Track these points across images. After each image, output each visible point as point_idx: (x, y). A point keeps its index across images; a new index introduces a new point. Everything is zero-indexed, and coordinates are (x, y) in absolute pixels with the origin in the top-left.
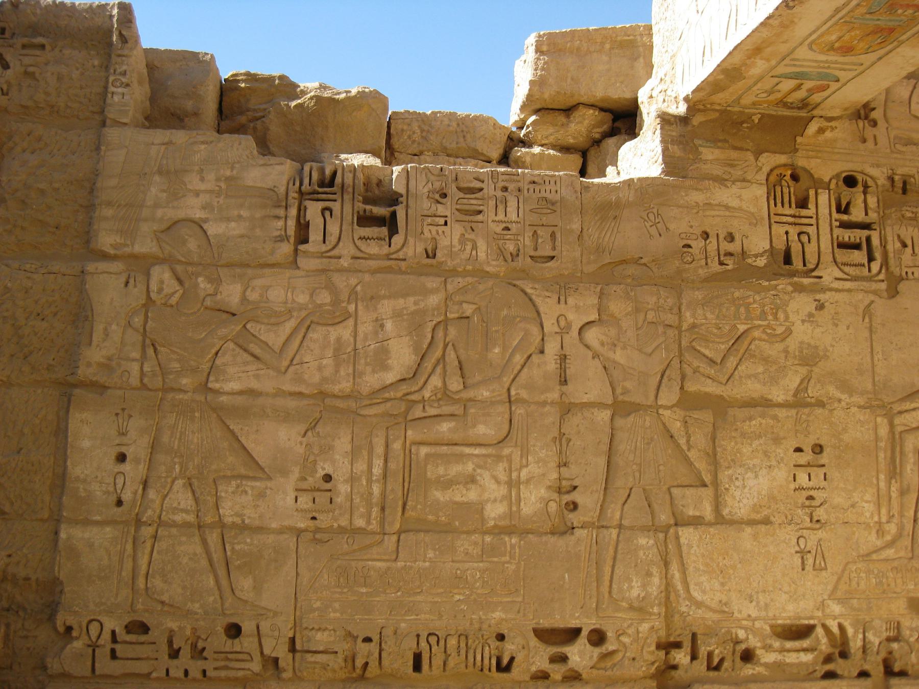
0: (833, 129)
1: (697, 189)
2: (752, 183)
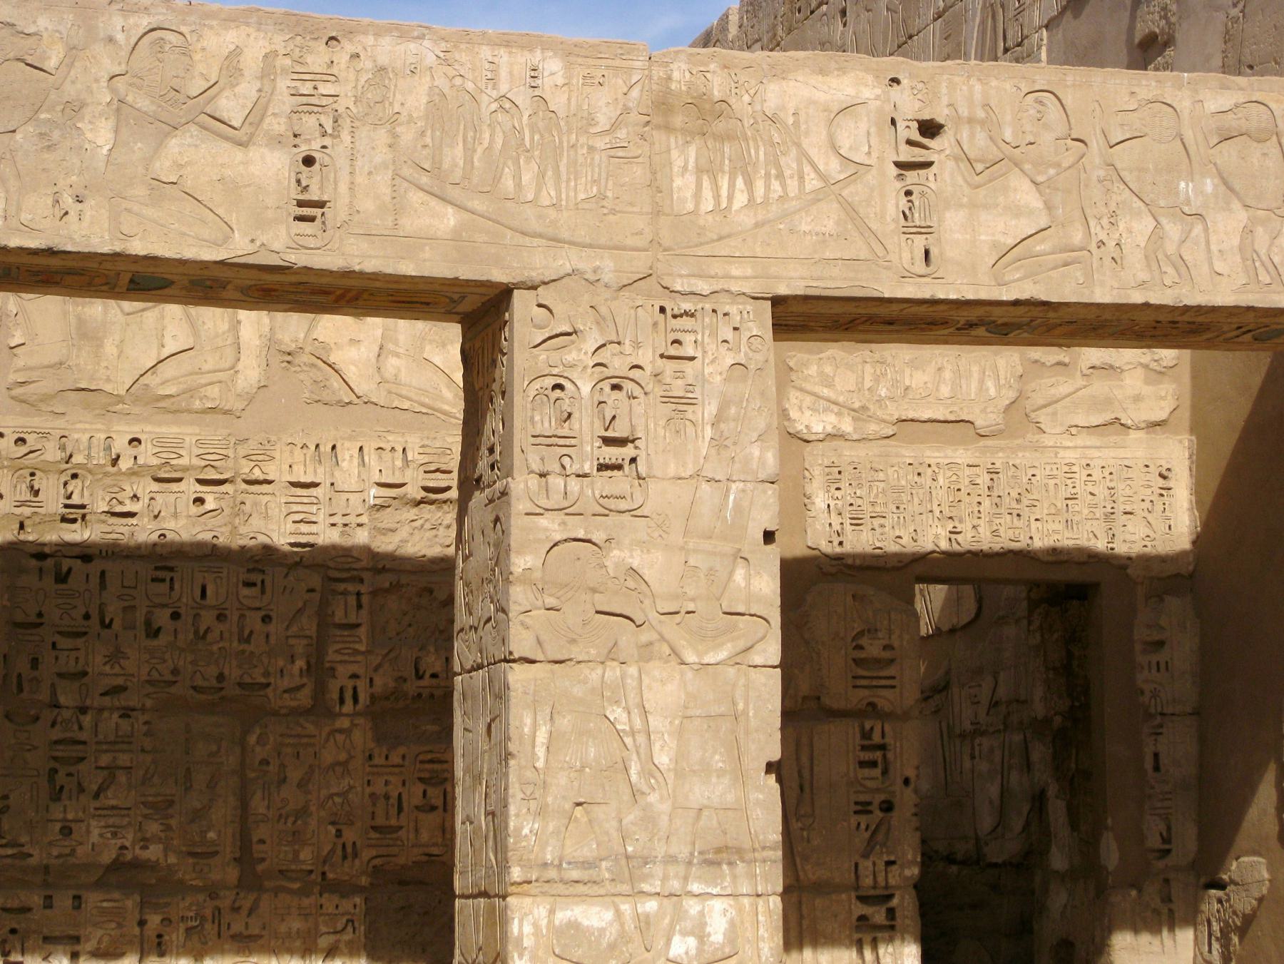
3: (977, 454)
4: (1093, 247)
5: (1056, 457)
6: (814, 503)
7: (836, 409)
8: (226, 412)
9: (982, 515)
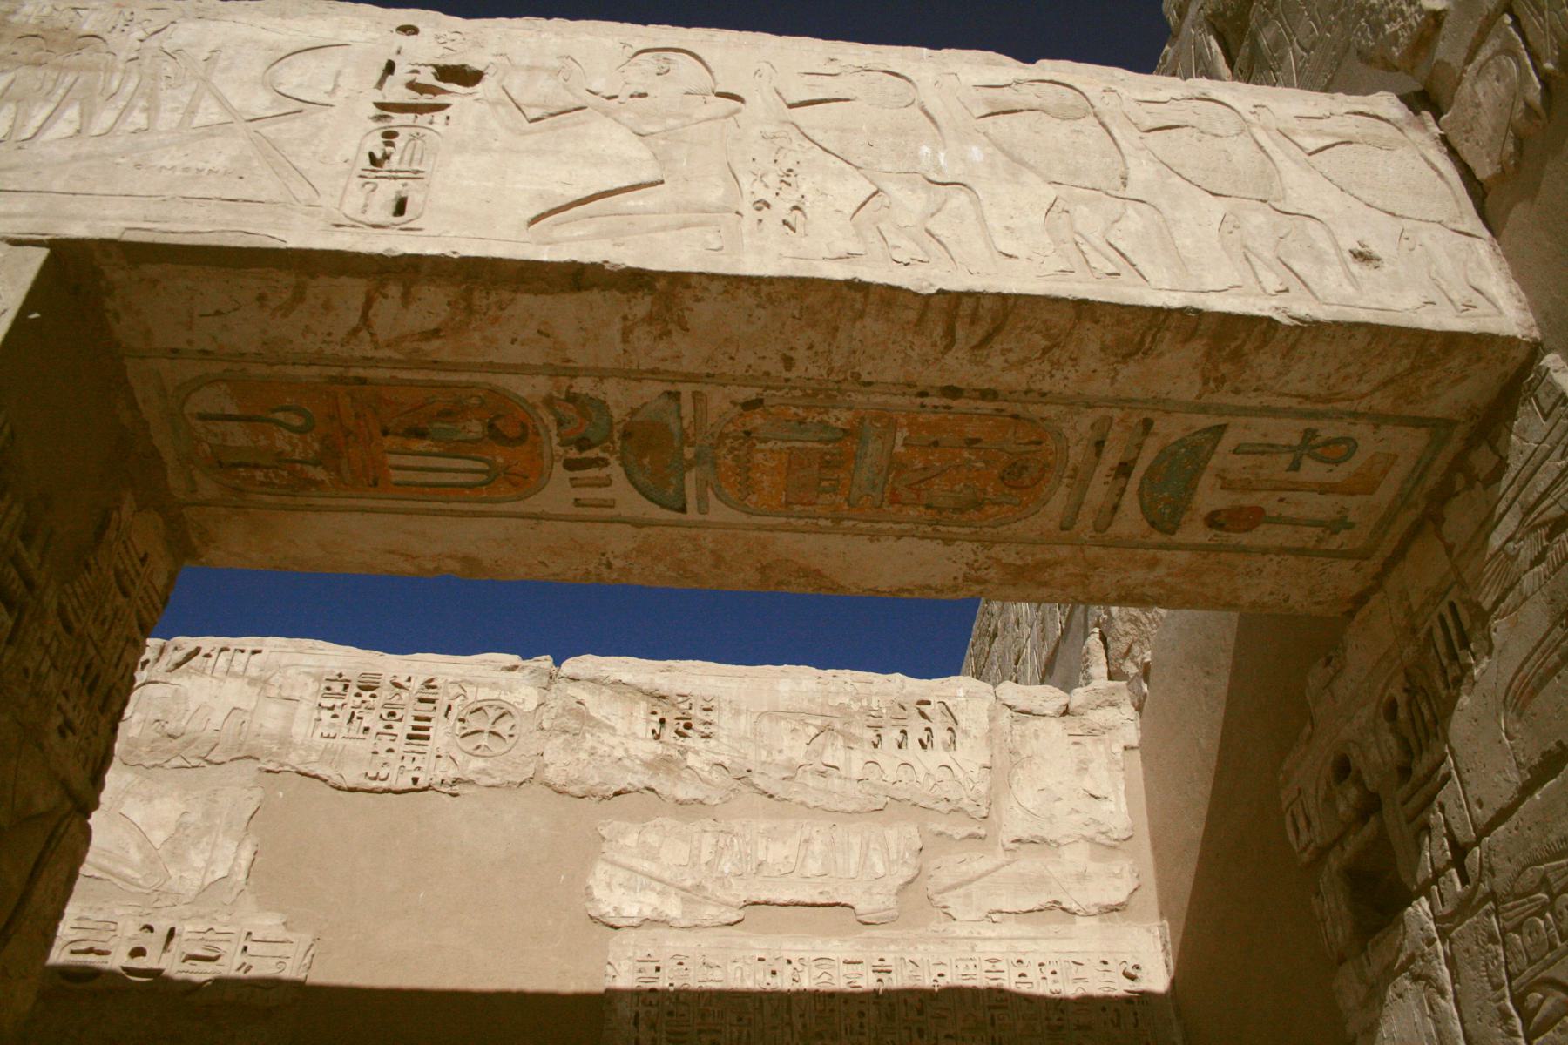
3: (858, 947)
4: (746, 207)
5: (973, 950)
6: (615, 1010)
7: (659, 887)
9: (866, 1030)
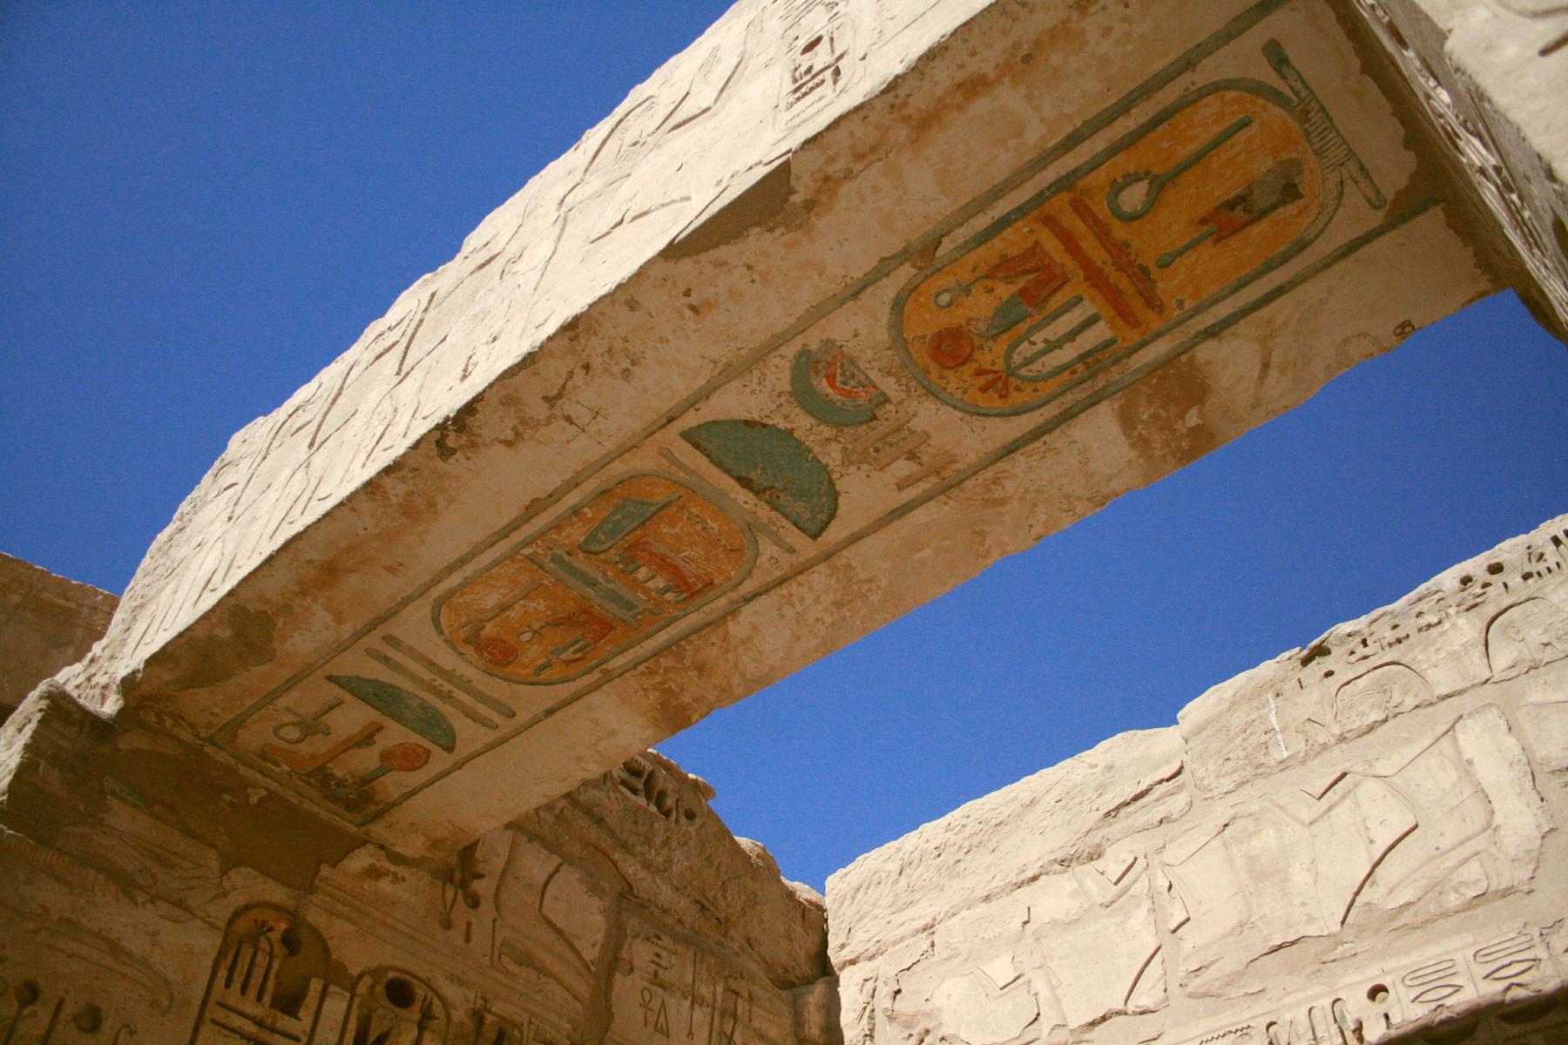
0: (396, 879)
1: (59, 879)
2: (195, 916)
8: (1506, 893)
